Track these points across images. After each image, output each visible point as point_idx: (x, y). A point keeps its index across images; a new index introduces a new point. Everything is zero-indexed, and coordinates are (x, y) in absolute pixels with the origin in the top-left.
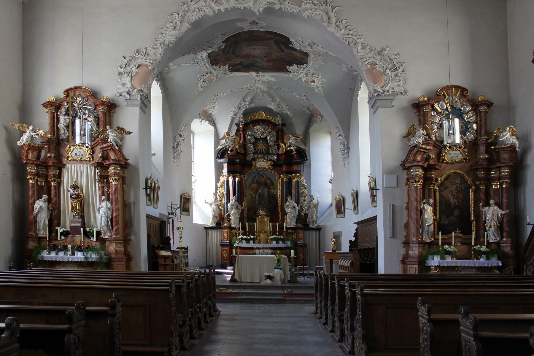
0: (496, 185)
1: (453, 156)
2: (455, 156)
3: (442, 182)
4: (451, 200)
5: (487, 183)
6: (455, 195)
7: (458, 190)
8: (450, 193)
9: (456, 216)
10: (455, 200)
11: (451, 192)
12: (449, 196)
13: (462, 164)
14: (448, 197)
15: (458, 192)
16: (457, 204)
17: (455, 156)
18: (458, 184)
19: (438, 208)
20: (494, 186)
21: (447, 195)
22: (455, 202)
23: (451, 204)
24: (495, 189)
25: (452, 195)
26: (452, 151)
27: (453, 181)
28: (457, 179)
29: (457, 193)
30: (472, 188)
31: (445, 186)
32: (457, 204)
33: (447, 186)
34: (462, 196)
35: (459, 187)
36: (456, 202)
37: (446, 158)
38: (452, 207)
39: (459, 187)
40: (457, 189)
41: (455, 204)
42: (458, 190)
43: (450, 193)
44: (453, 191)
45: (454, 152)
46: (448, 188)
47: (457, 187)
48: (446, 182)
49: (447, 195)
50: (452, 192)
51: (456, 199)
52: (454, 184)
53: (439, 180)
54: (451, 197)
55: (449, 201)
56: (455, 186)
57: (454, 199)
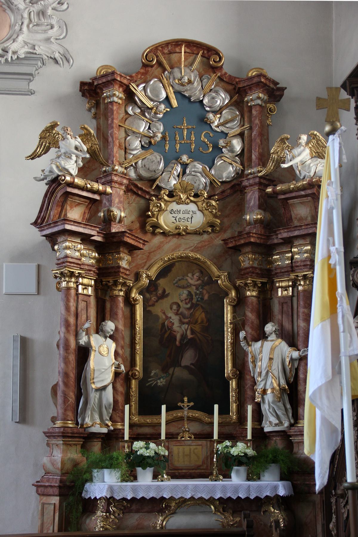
0: (285, 288)
1: (181, 216)
2: (186, 216)
3: (151, 281)
4: (176, 327)
5: (262, 283)
6: (186, 313)
7: (194, 301)
8: (171, 309)
9: (186, 367)
10: (187, 326)
11: (175, 307)
12: (169, 315)
13: (205, 236)
14: (167, 318)
15: (193, 306)
16: (189, 336)
17: (186, 216)
18: (194, 288)
19: (139, 348)
20: (280, 290)
21: (164, 313)
22: (186, 331)
23: (176, 340)
24: (283, 297)
25: (177, 314)
26: (178, 203)
27: (179, 280)
28: (190, 275)
29: (189, 309)
30: (230, 296)
31: (160, 292)
32: (189, 336)
33: (164, 291)
34: (203, 315)
35: (196, 294)
36: (189, 332)
37: (161, 221)
38: (177, 343)
39: (196, 294)
40: (192, 299)
41: (184, 336)
42: (194, 301)
43: (171, 309)
44: (180, 303)
45: (182, 207)
46: (168, 295)
47: (190, 294)
48: (162, 282)
49: (164, 313)
50: (179, 306)
51: (187, 323)
52: (183, 287)
53: (144, 275)
54: (175, 319)
55: (170, 329)
56: (186, 292)
57: (184, 323)
